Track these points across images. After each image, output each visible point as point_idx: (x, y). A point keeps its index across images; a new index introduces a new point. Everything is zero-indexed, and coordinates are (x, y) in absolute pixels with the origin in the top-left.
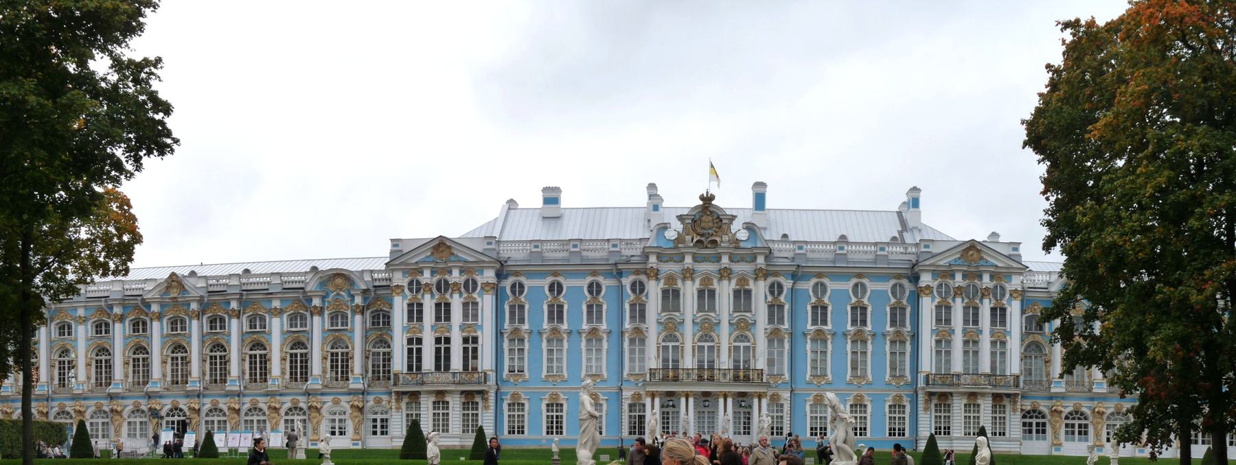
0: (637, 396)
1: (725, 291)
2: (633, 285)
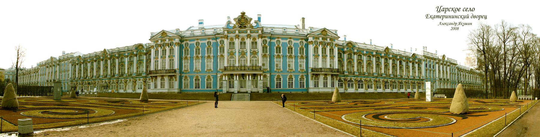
0: (222, 76)
1: (248, 42)
2: (221, 41)
